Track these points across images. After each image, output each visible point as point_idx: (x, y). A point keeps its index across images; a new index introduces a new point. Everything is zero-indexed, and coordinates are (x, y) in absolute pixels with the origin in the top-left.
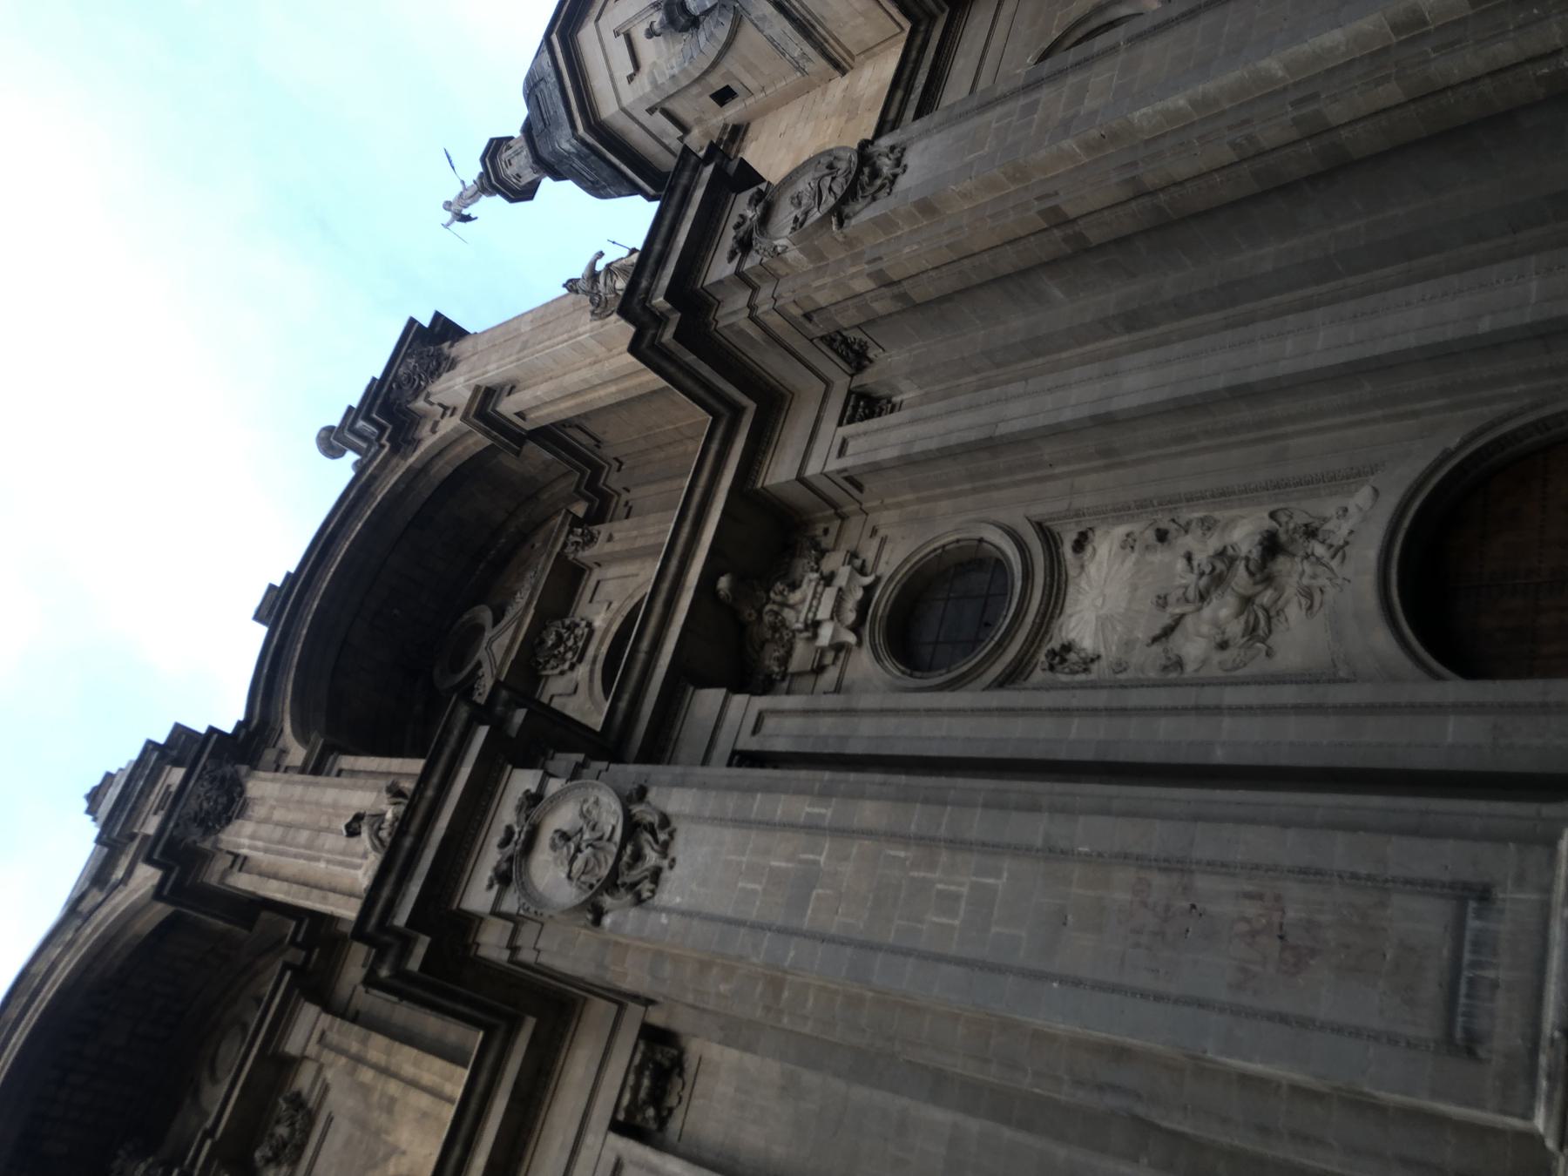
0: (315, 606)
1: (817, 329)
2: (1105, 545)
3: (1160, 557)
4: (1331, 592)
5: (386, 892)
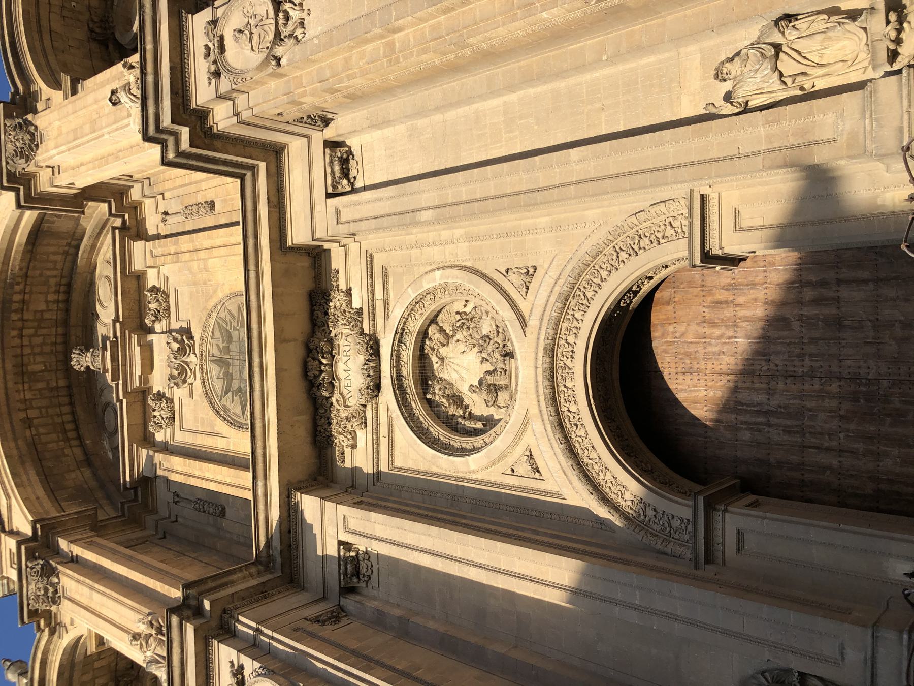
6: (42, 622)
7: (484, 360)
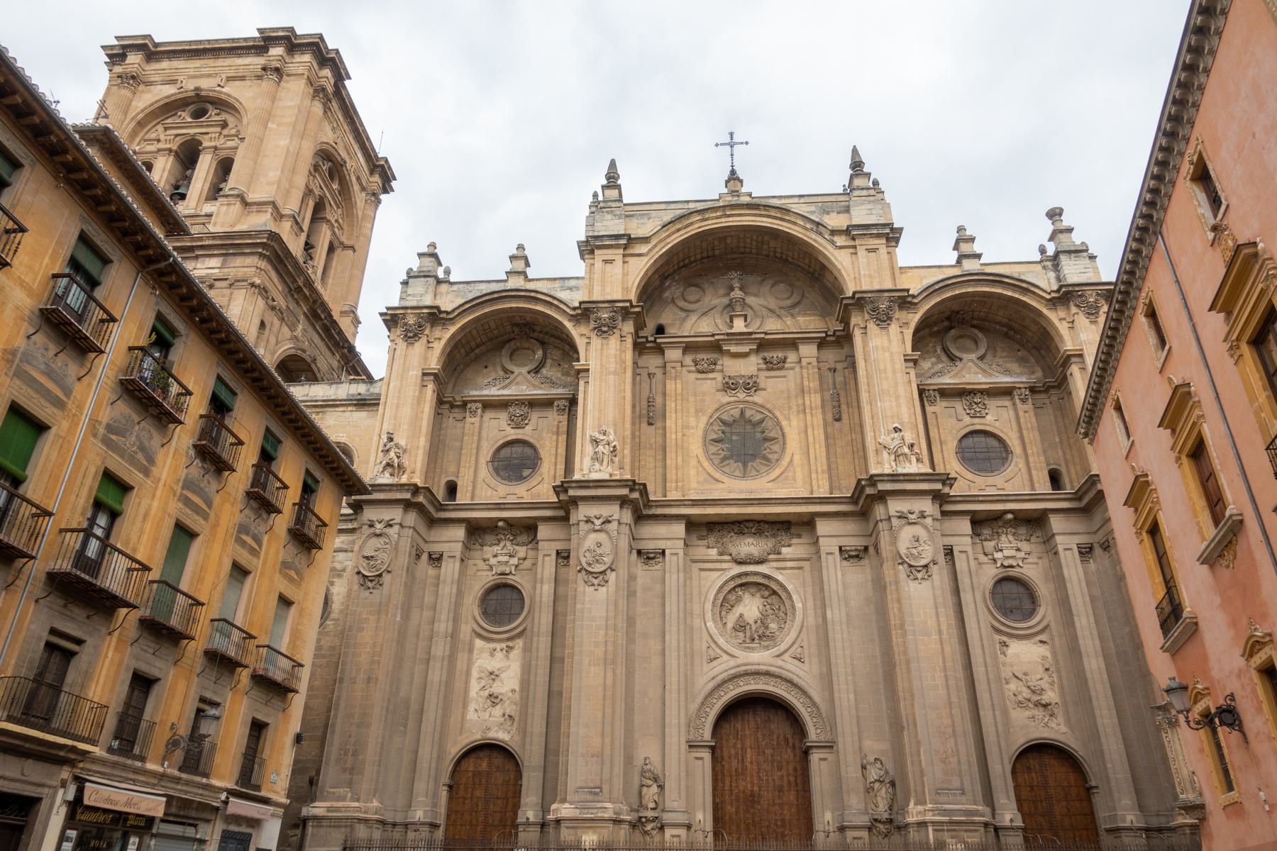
0: (970, 290)
1: (1110, 538)
2: (1044, 651)
3: (1041, 669)
4: (1033, 724)
5: (886, 478)
6: (579, 311)
7: (756, 622)
